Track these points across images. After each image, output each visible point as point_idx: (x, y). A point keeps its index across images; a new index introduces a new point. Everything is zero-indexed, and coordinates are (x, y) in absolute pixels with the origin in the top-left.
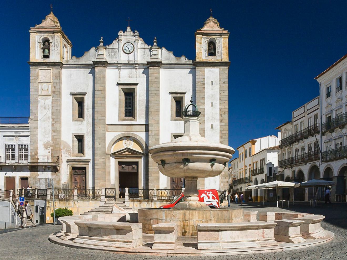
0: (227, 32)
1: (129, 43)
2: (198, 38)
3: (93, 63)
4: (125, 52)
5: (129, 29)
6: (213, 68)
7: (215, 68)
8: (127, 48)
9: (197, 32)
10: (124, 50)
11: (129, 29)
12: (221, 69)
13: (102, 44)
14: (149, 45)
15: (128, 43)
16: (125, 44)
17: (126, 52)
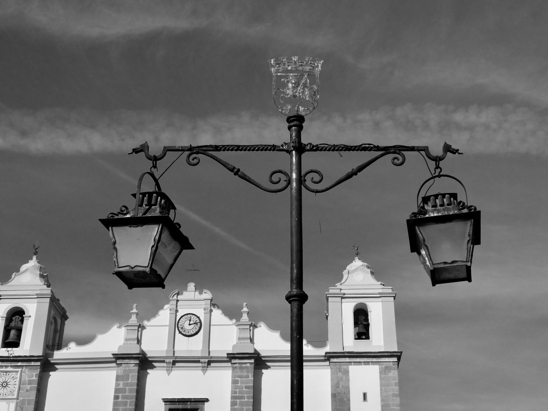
0: (390, 291)
1: (191, 315)
2: (333, 303)
3: (112, 356)
4: (183, 332)
5: (191, 286)
6: (365, 365)
7: (369, 364)
8: (187, 326)
9: (331, 291)
10: (181, 330)
11: (191, 286)
12: (384, 366)
13: (134, 318)
14: (231, 319)
15: (189, 316)
16: (182, 317)
17: (185, 333)
